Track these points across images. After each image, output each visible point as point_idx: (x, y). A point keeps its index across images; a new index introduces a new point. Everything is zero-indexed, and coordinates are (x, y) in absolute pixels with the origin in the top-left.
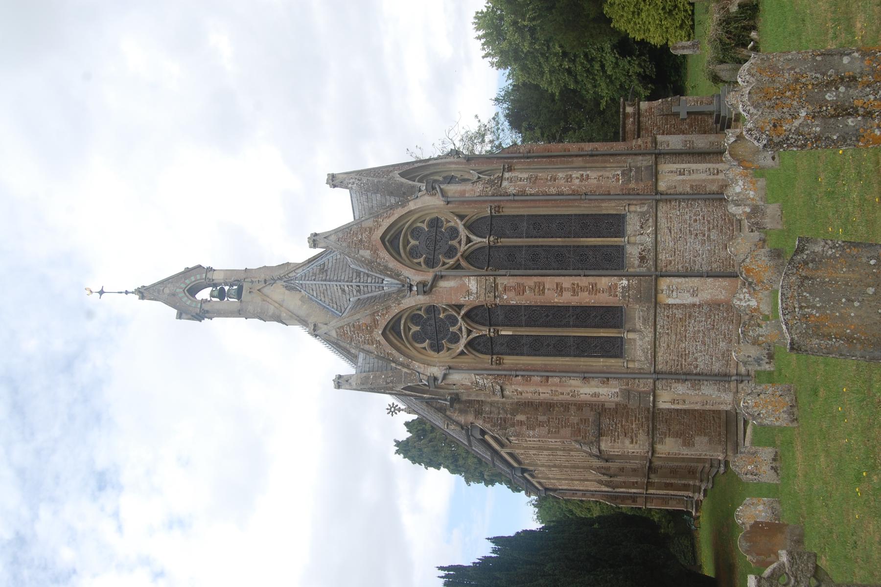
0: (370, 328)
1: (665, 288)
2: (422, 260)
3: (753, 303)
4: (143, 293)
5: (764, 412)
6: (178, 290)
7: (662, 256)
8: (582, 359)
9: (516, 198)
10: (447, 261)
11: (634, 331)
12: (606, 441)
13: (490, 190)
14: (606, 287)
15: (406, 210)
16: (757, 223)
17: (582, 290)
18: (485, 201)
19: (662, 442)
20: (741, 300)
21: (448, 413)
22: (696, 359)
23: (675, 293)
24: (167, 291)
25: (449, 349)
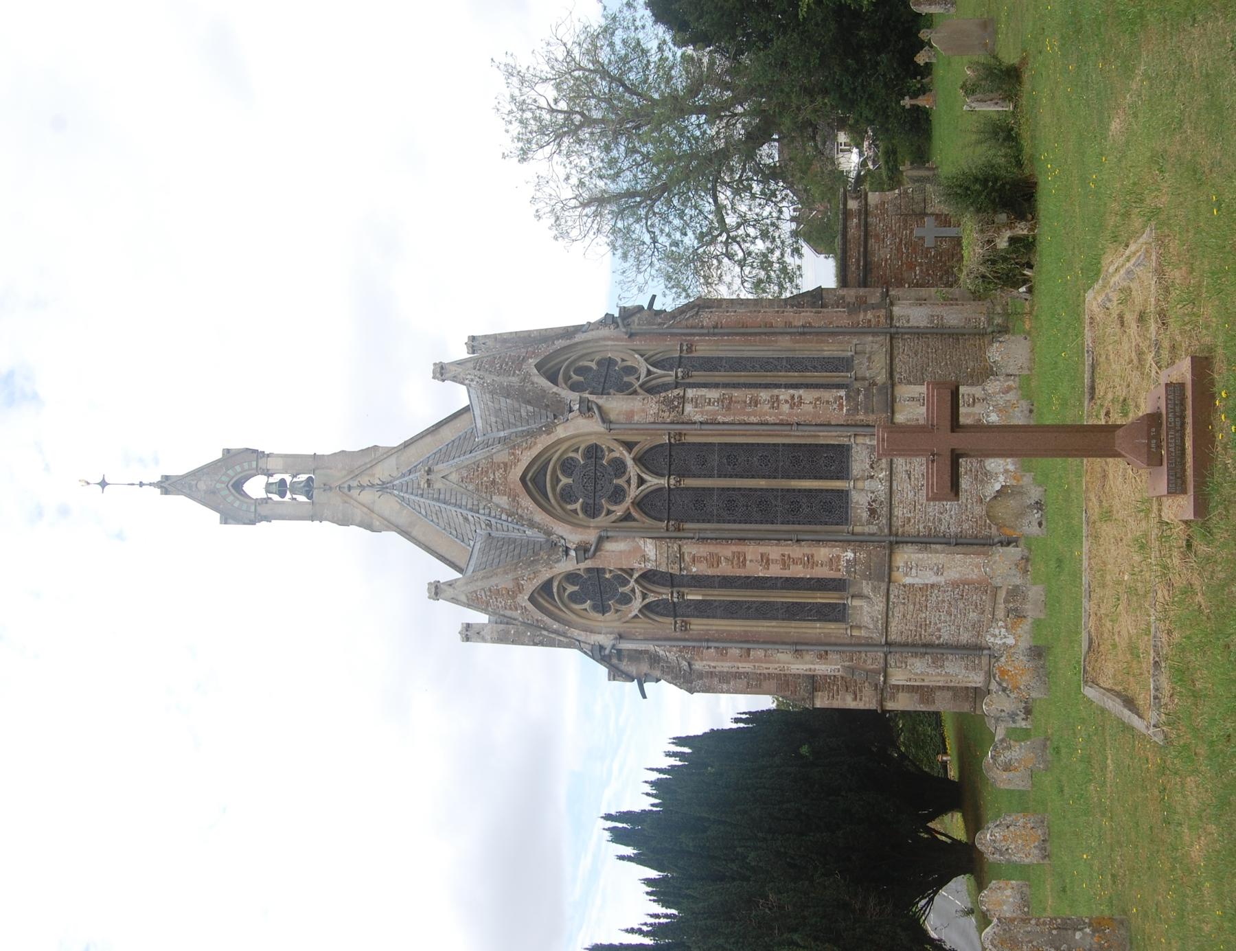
0: (513, 593)
1: (901, 564)
2: (578, 506)
3: (1011, 641)
4: (168, 485)
5: (1013, 846)
6: (219, 486)
7: (898, 512)
8: (793, 624)
9: (704, 427)
10: (612, 508)
11: (860, 596)
12: (822, 698)
13: (668, 416)
14: (825, 559)
15: (551, 439)
16: (1016, 610)
17: (795, 562)
20: (995, 636)
22: (939, 630)
23: (914, 571)
24: (202, 486)
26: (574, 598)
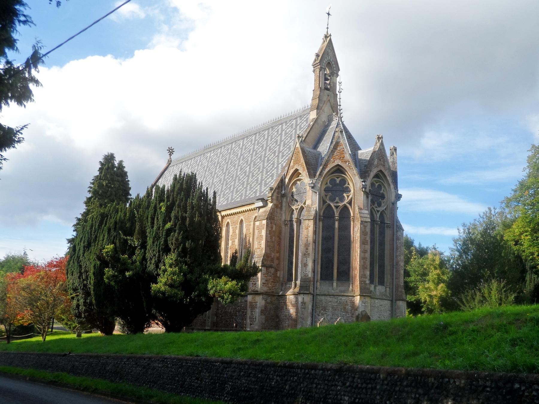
18: (394, 221)
19: (263, 299)
21: (277, 190)
24: (329, 51)
25: (326, 196)
26: (333, 181)
